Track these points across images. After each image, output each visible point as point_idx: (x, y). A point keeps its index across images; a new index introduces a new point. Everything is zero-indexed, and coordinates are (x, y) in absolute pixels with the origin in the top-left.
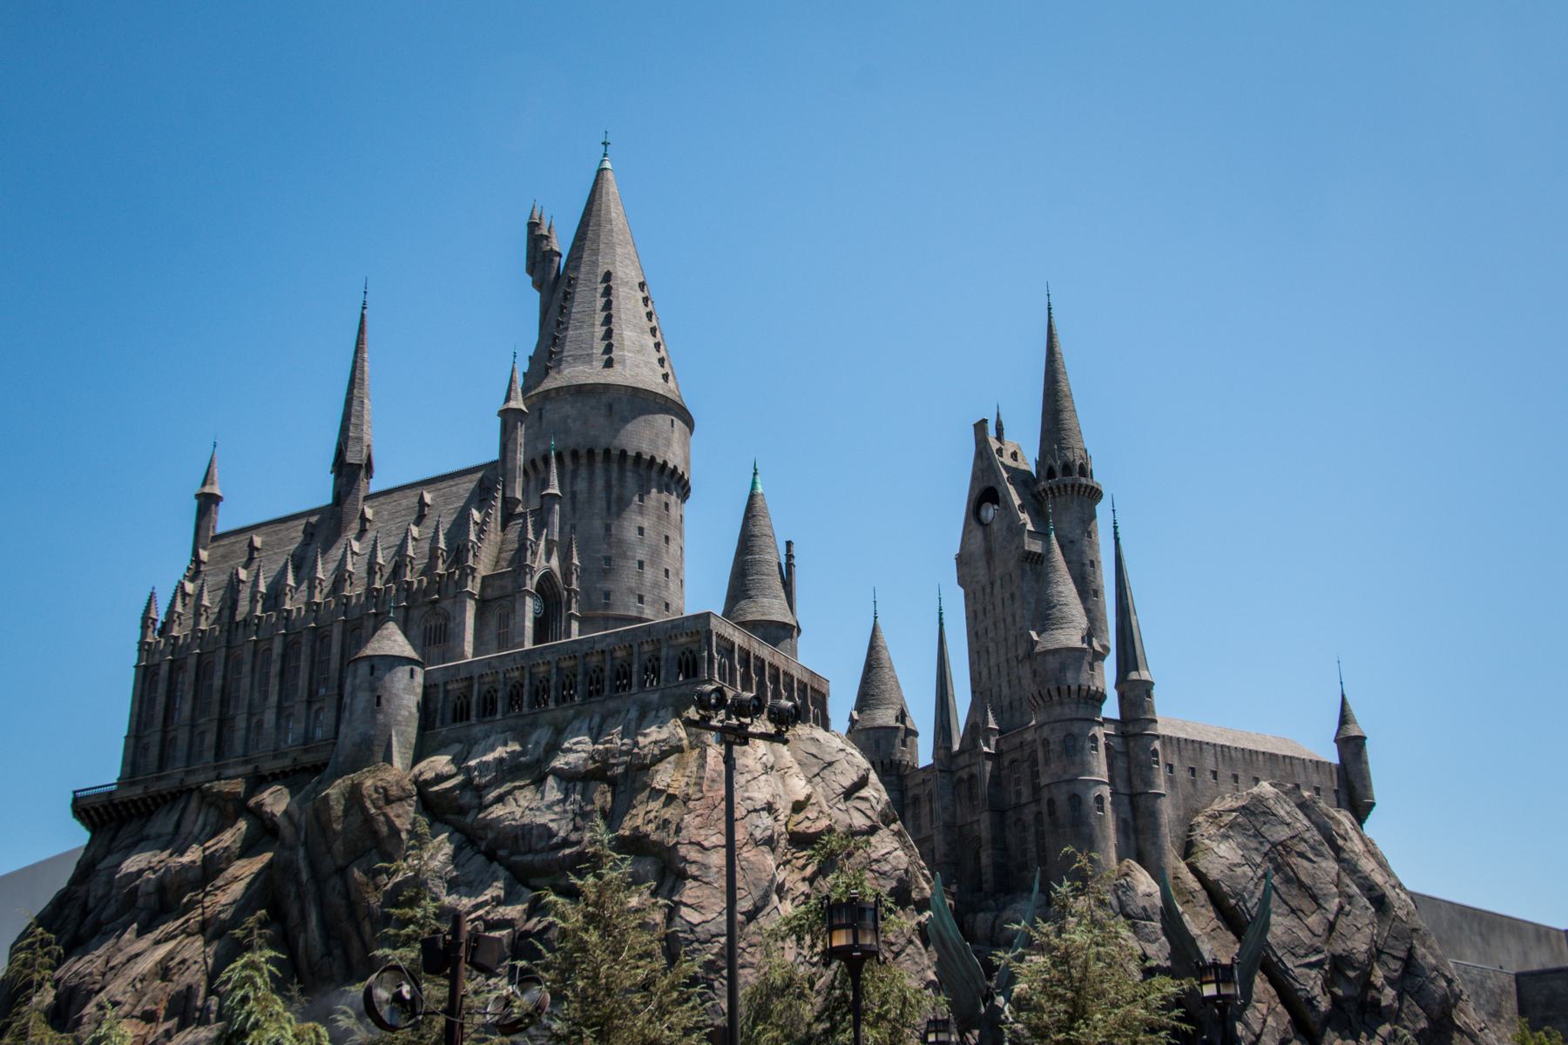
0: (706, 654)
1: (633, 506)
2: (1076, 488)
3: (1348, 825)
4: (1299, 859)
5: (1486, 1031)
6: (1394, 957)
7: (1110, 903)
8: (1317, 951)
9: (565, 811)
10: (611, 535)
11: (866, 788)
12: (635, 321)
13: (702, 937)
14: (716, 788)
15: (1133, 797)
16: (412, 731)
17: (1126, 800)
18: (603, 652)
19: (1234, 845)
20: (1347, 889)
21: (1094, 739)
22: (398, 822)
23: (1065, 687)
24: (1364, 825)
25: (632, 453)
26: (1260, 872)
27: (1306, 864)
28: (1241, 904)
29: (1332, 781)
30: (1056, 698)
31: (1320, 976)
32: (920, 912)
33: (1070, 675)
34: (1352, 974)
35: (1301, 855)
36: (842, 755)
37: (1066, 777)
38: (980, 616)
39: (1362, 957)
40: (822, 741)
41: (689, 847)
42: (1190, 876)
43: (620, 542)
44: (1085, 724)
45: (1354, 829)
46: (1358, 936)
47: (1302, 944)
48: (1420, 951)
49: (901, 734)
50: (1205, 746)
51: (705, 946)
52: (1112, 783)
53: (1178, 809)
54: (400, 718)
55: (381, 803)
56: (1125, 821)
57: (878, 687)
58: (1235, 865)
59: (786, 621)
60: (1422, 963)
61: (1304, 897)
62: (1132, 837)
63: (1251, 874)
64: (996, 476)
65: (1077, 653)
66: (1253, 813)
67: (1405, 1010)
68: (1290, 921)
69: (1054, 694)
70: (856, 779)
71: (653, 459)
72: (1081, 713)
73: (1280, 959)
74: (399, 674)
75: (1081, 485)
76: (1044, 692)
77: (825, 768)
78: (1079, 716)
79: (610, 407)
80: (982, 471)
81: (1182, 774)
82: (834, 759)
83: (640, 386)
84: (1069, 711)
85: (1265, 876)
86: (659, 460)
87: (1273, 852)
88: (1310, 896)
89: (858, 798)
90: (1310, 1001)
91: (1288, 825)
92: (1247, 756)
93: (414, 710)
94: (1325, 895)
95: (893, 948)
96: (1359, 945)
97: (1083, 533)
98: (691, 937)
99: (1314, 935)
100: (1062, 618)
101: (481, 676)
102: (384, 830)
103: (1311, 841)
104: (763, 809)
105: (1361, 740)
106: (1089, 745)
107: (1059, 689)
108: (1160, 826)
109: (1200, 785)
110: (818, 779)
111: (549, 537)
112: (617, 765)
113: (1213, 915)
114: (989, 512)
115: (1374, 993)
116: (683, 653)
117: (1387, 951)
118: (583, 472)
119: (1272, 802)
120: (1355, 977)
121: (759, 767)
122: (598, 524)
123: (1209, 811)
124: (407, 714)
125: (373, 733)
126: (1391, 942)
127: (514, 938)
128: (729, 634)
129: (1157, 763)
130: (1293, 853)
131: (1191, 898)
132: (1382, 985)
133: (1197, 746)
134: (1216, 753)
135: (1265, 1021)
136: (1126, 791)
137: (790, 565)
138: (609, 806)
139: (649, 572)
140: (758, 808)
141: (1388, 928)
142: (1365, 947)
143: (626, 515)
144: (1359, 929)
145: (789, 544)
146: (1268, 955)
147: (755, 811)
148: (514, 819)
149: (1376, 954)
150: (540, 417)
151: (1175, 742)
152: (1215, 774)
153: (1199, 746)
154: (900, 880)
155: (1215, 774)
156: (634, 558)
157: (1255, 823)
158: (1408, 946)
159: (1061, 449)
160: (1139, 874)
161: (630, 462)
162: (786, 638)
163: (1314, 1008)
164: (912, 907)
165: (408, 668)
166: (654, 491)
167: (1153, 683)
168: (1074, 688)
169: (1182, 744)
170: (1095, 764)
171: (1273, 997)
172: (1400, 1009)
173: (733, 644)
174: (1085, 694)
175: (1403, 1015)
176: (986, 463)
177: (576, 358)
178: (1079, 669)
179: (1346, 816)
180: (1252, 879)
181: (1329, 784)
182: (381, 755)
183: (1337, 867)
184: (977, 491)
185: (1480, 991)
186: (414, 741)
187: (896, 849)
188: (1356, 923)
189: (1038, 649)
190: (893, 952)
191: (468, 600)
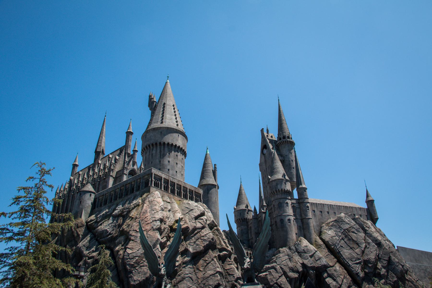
0: (150, 179)
2: (287, 142)
3: (370, 224)
4: (352, 233)
5: (419, 281)
6: (385, 260)
7: (293, 249)
8: (359, 259)
9: (112, 226)
10: (161, 163)
11: (204, 216)
12: (170, 113)
13: (131, 257)
14: (144, 215)
15: (302, 220)
16: (89, 210)
17: (300, 221)
18: (129, 183)
19: (333, 231)
20: (368, 241)
21: (287, 203)
22: (79, 233)
23: (278, 190)
24: (376, 225)
25: (166, 143)
26: (341, 238)
27: (355, 234)
28: (335, 247)
29: (365, 212)
30: (276, 193)
31: (360, 266)
32: (220, 252)
33: (279, 186)
34: (370, 265)
35: (353, 232)
36: (196, 207)
37: (279, 214)
38: (265, 178)
39: (373, 260)
40: (190, 204)
41: (133, 231)
42: (320, 240)
43: (163, 164)
44: (284, 199)
45: (372, 225)
46: (371, 254)
47: (354, 257)
48: (393, 258)
49: (247, 211)
50: (324, 205)
51: (131, 260)
52: (295, 215)
53: (317, 222)
54: (86, 206)
55: (76, 228)
56: (300, 226)
57: (241, 200)
58: (333, 236)
59: (214, 184)
60: (394, 261)
61: (354, 244)
62: (302, 231)
63: (338, 239)
64: (266, 142)
65: (281, 180)
66: (338, 222)
67: (390, 275)
68: (350, 251)
69: (275, 192)
70: (199, 213)
71: (172, 144)
72: (283, 197)
73: (347, 262)
74: (87, 195)
75: (288, 141)
76: (272, 192)
77: (190, 211)
78: (282, 197)
79: (161, 132)
80: (263, 141)
81: (318, 213)
82: (193, 208)
83: (169, 127)
84: (279, 196)
85: (343, 239)
86: (174, 144)
87: (344, 232)
88: (356, 244)
89: (200, 219)
90: (357, 274)
92: (338, 207)
93: (90, 204)
94: (361, 243)
95: (207, 262)
96: (372, 257)
97: (289, 153)
98: (128, 257)
100: (277, 172)
101: (106, 194)
102: (76, 235)
103: (356, 228)
104: (158, 220)
105: (372, 201)
106: (285, 205)
107: (276, 191)
108: (310, 227)
109: (323, 215)
110: (188, 214)
111: (133, 161)
112: (125, 212)
113: (327, 251)
114: (265, 151)
115: (378, 270)
116: (146, 180)
117: (383, 258)
118: (155, 149)
119: (343, 218)
120: (371, 266)
121: (160, 209)
122: (157, 161)
123: (326, 222)
124: (88, 205)
125: (78, 210)
126: (383, 255)
127: (93, 261)
128: (160, 175)
129: (309, 210)
130: (351, 232)
131: (320, 246)
132: (381, 268)
133: (322, 205)
134: (328, 207)
135: (343, 281)
136: (300, 218)
137: (215, 170)
138: (121, 223)
140: (156, 220)
141: (382, 252)
142: (374, 257)
143: (165, 158)
144: (372, 252)
145: (215, 165)
146: (344, 261)
147: (155, 221)
148: (101, 229)
149: (378, 258)
150: (146, 137)
151: (315, 204)
152: (328, 212)
153: (323, 205)
154: (210, 242)
155: (328, 212)
156: (167, 168)
157: (339, 224)
158: (389, 256)
159: (282, 133)
160: (303, 241)
162: (213, 188)
163: (359, 276)
164: (217, 250)
165: (89, 194)
166: (173, 152)
167: (306, 189)
168: (280, 190)
169: (318, 205)
170: (287, 210)
171: (346, 273)
172: (388, 275)
173: (162, 177)
175: (389, 277)
176: (264, 139)
177: (154, 123)
178: (281, 184)
179: (370, 222)
180: (338, 240)
181: (364, 214)
182: (80, 216)
183: (364, 235)
184: (262, 146)
185: (426, 272)
186: (89, 212)
187: (209, 233)
188: (371, 250)
189: (271, 180)
190: (206, 263)
191: (110, 177)
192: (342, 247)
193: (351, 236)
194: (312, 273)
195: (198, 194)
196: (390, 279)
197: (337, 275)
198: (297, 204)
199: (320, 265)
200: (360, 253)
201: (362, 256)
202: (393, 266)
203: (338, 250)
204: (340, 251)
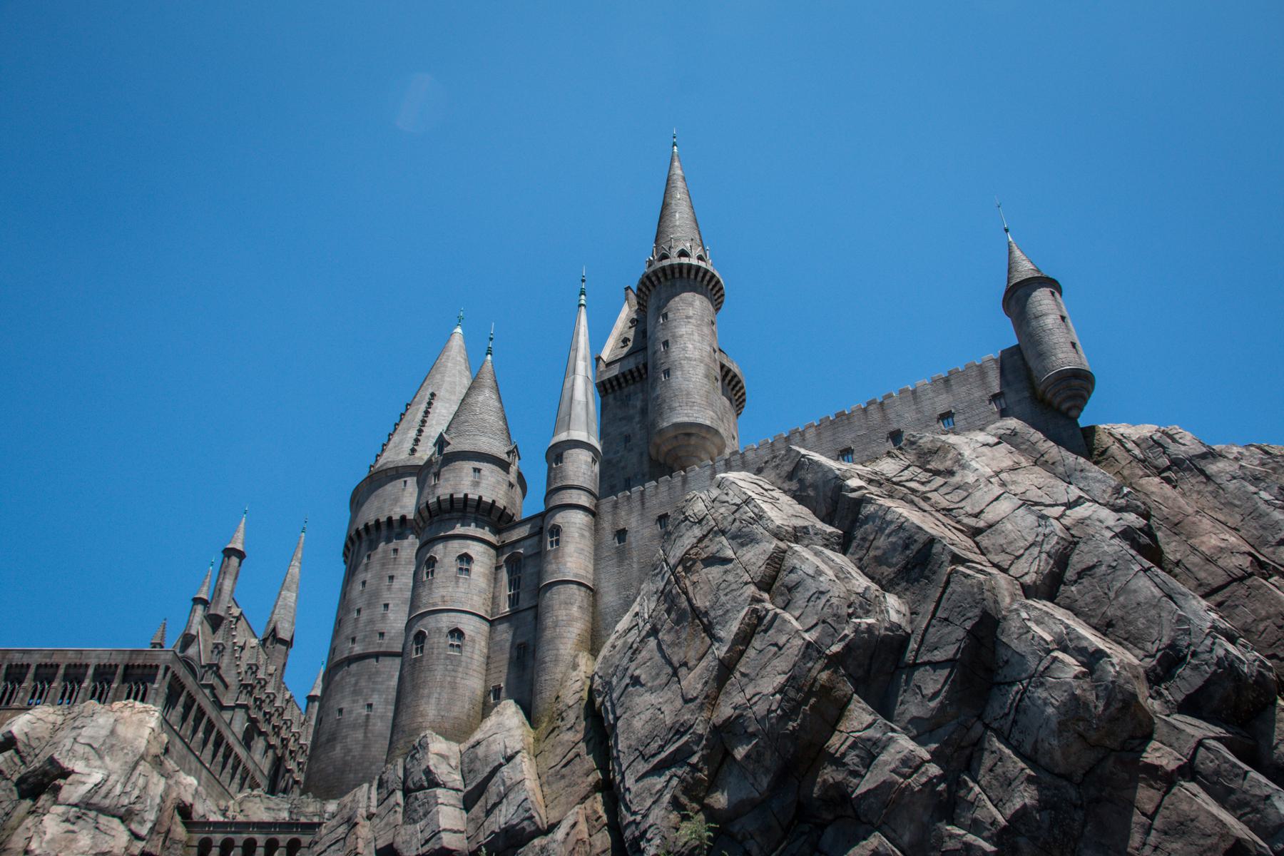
1: (362, 567)
6: (935, 665)
85: (654, 632)
86: (383, 519)
117: (925, 658)
120: (747, 756)
130: (699, 565)
139: (364, 616)
161: (363, 534)
174: (426, 514)
192: (636, 681)
193: (690, 589)
195: (147, 671)
196: (979, 814)
200: (700, 686)
201: (711, 701)
202: (1015, 688)
203: (614, 712)
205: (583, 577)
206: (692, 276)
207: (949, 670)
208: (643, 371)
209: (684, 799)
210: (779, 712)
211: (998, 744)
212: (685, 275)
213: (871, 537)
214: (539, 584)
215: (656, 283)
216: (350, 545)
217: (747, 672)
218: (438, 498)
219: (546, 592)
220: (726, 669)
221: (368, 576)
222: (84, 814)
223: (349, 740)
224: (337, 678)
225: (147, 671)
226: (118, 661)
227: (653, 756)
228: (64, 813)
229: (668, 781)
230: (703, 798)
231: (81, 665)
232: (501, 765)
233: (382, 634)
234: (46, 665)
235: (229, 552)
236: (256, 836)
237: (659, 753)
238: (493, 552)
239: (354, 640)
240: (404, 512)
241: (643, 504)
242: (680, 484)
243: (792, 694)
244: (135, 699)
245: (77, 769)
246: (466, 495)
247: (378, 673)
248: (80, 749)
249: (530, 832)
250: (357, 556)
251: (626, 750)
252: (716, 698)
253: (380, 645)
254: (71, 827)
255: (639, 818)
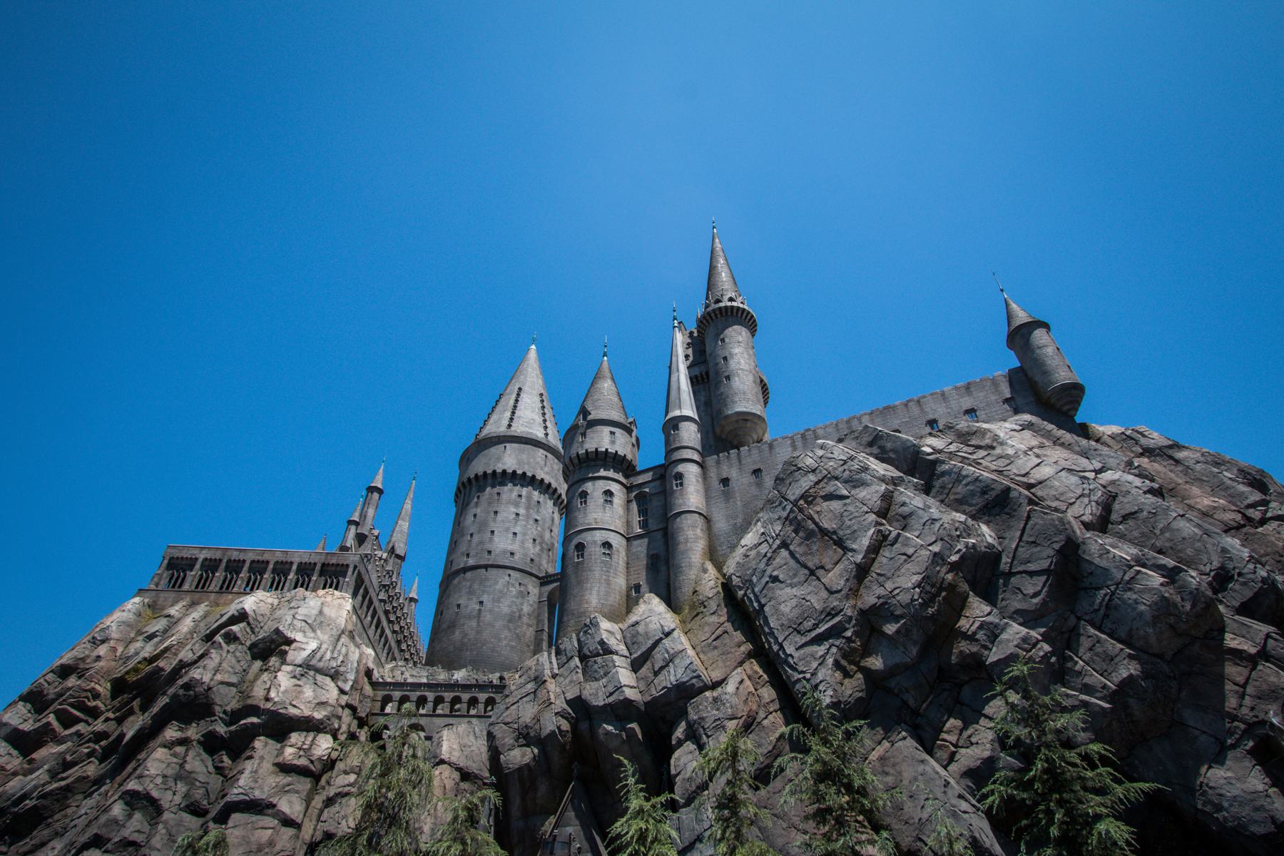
1: (473, 504)
6: (1032, 574)
26: (778, 542)
34: (890, 629)
60: (1104, 564)
62: (664, 568)
71: (485, 473)
85: (784, 545)
86: (489, 471)
88: (836, 543)
91: (814, 471)
94: (855, 531)
99: (831, 592)
117: (1020, 569)
120: (898, 632)
128: (192, 554)
130: (819, 500)
131: (702, 609)
139: (476, 539)
144: (909, 557)
146: (769, 643)
161: (474, 482)
174: (576, 461)
192: (775, 579)
193: (816, 516)
194: (608, 733)
195: (338, 569)
196: (1087, 680)
197: (715, 721)
198: (658, 483)
199: (662, 689)
200: (842, 582)
201: (854, 592)
202: (1103, 592)
203: (758, 601)
204: (763, 601)
205: (700, 509)
206: (739, 315)
207: (1046, 577)
208: (705, 377)
209: (844, 663)
210: (920, 600)
211: (1092, 631)
212: (735, 314)
213: (950, 486)
214: (666, 514)
215: (714, 318)
216: (462, 489)
217: (883, 572)
218: (587, 450)
219: (676, 518)
220: (862, 572)
221: (478, 511)
222: (306, 672)
223: (465, 627)
224: (455, 582)
225: (338, 569)
226: (316, 561)
227: (809, 631)
228: (292, 671)
229: (829, 649)
230: (859, 662)
231: (286, 562)
232: (661, 639)
233: (489, 552)
234: (258, 561)
235: (372, 489)
236: (427, 694)
237: (815, 629)
238: (625, 490)
239: (468, 555)
240: (505, 467)
241: (740, 461)
242: (767, 449)
243: (928, 588)
244: (330, 587)
245: (297, 639)
246: (607, 449)
247: (487, 579)
248: (299, 624)
249: (699, 687)
250: (469, 497)
251: (779, 628)
252: (858, 590)
253: (489, 560)
254: (298, 682)
255: (808, 676)
